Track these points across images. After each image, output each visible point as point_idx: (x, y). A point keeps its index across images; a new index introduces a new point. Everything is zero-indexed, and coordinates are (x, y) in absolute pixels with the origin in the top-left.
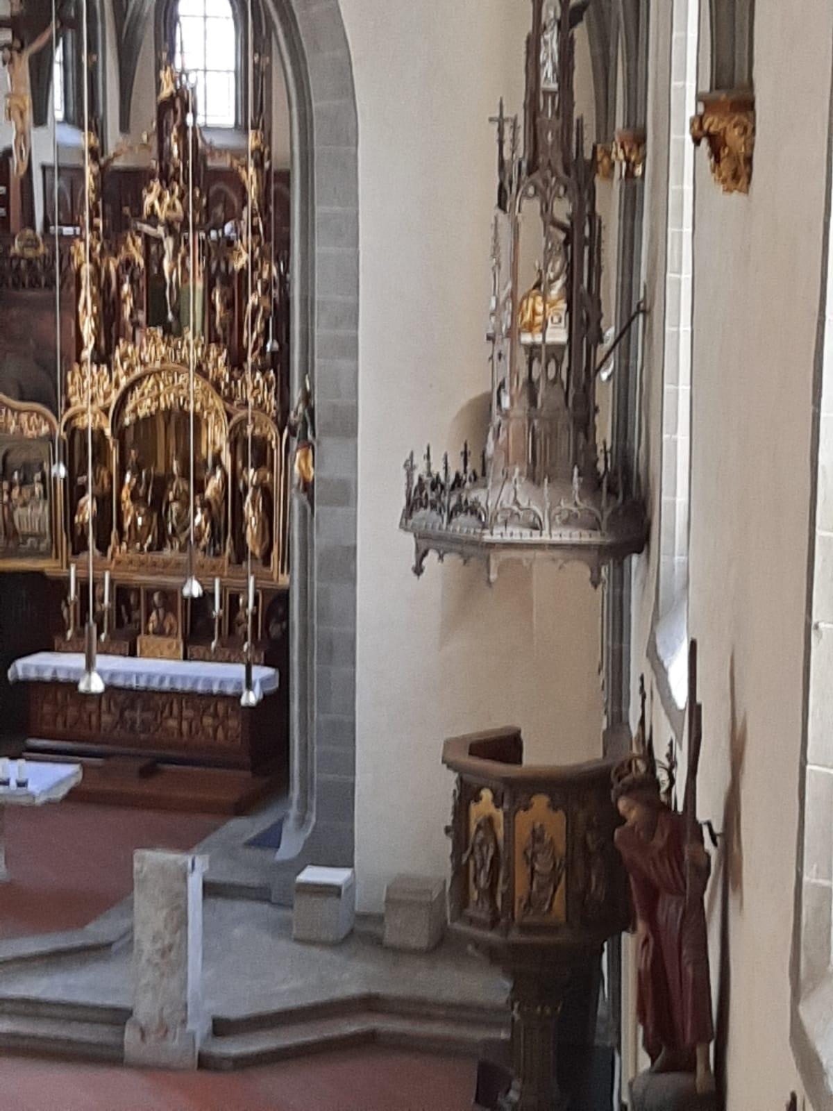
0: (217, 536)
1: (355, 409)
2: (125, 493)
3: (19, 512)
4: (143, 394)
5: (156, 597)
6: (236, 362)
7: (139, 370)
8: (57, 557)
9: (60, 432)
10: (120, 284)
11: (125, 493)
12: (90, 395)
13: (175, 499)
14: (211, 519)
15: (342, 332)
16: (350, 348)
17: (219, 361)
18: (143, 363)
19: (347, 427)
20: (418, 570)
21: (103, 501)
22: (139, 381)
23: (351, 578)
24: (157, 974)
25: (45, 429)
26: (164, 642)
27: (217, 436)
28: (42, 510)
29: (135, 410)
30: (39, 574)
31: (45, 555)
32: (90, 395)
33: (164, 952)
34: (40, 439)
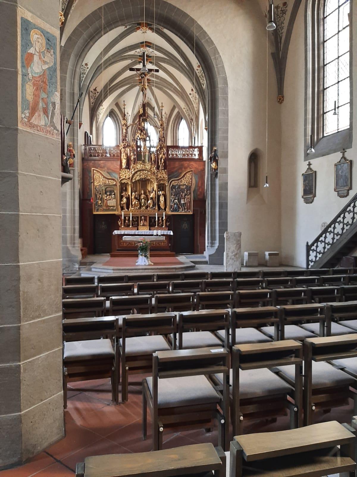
0: (154, 205)
1: (227, 152)
3: (108, 202)
4: (137, 175)
5: (143, 217)
6: (158, 168)
7: (136, 170)
9: (118, 184)
13: (143, 199)
15: (224, 135)
16: (226, 138)
18: (137, 169)
21: (128, 199)
22: (136, 172)
23: (227, 190)
24: (233, 261)
26: (145, 227)
28: (114, 200)
29: (135, 179)
30: (114, 214)
31: (115, 210)
33: (235, 255)
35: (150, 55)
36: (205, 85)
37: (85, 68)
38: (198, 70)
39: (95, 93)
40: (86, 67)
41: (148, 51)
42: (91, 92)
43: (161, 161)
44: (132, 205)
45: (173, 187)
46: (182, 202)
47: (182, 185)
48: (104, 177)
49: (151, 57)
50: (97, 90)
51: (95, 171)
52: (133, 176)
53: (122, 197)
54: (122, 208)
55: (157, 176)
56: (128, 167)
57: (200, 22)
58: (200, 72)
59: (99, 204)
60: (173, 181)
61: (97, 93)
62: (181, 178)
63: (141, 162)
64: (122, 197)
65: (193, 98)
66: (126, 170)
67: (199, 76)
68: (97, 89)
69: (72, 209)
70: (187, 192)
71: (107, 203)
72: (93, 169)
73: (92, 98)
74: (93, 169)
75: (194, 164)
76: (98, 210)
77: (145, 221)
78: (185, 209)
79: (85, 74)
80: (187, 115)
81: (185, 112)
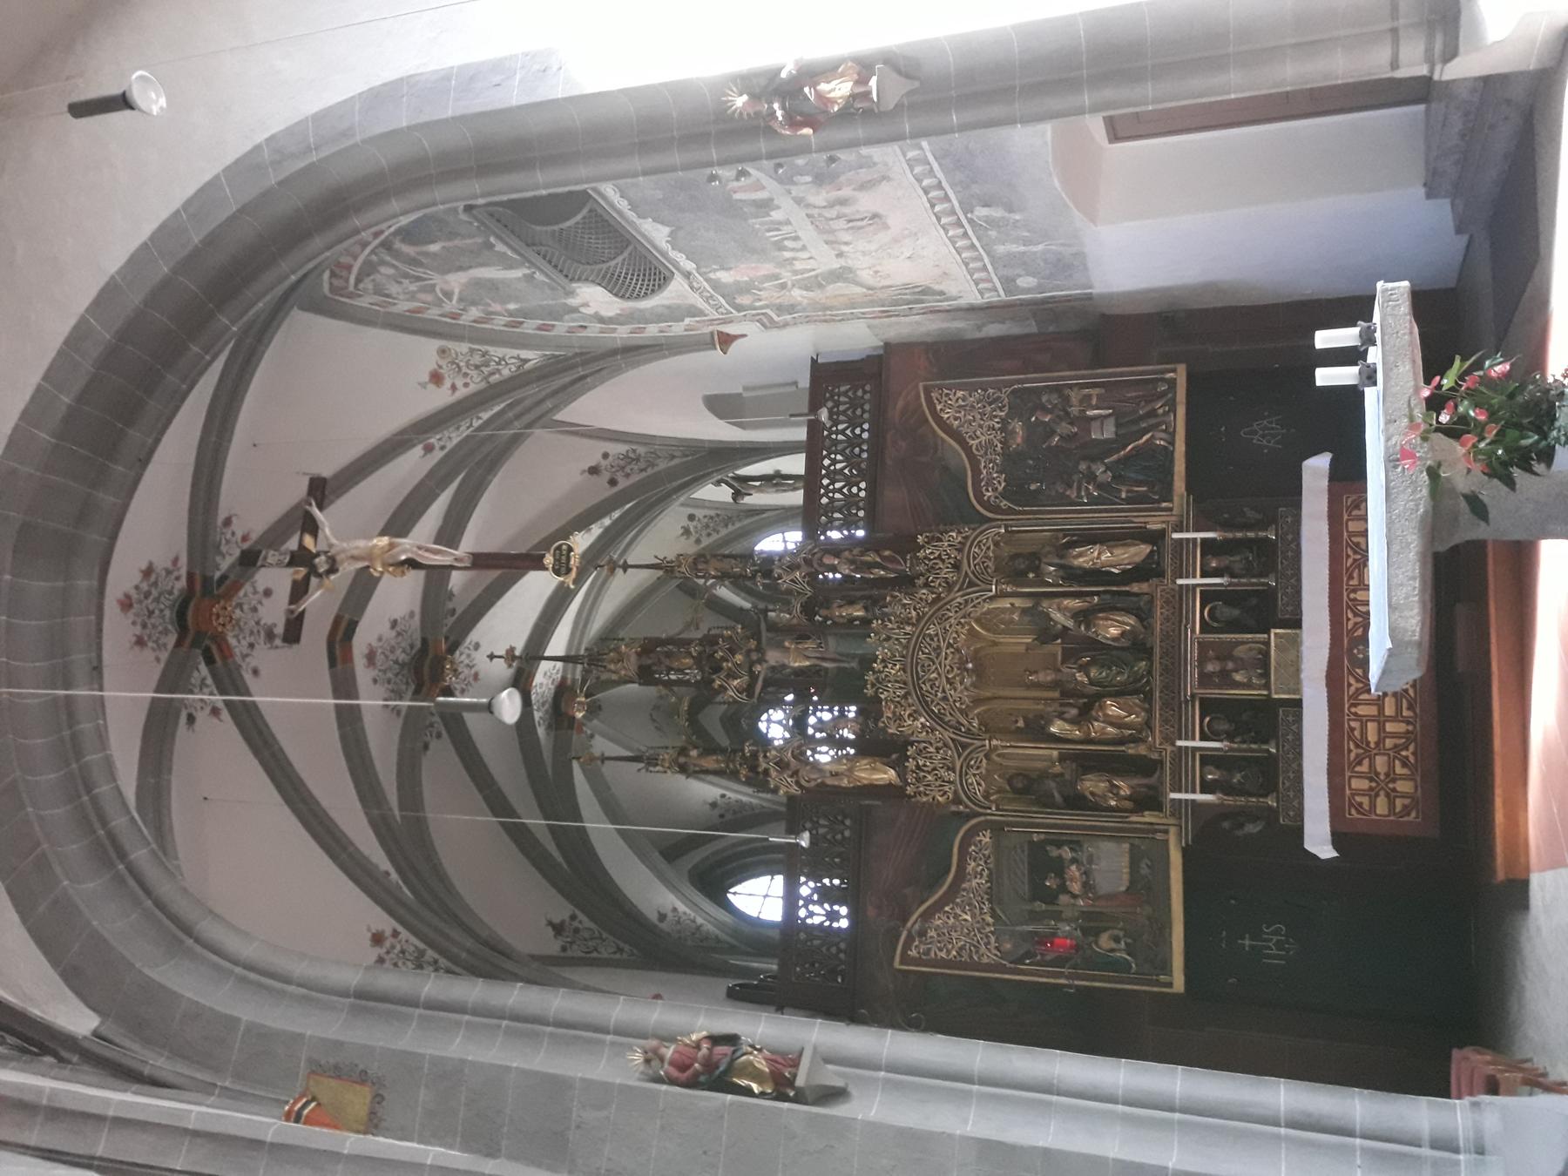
6: (906, 583)
17: (902, 604)
25: (986, 838)
34: (997, 846)
35: (418, 644)
36: (524, 354)
37: (393, 947)
38: (454, 388)
39: (577, 931)
40: (387, 944)
41: (393, 650)
42: (569, 953)
43: (870, 566)
44: (1121, 741)
45: (1018, 493)
46: (1109, 432)
47: (1004, 443)
48: (949, 897)
49: (424, 641)
50: (563, 922)
51: (913, 953)
53: (1077, 802)
55: (949, 586)
57: (114, 259)
58: (466, 375)
59: (1123, 945)
60: (979, 495)
61: (576, 924)
62: (967, 449)
63: (870, 677)
64: (1077, 802)
65: (628, 470)
66: (911, 764)
67: (483, 385)
68: (557, 920)
69: (1125, 1118)
70: (1046, 411)
71: (1111, 897)
72: (902, 963)
74: (897, 965)
75: (900, 404)
76: (1166, 967)
78: (1152, 414)
79: (422, 953)
80: (724, 532)
81: (715, 537)
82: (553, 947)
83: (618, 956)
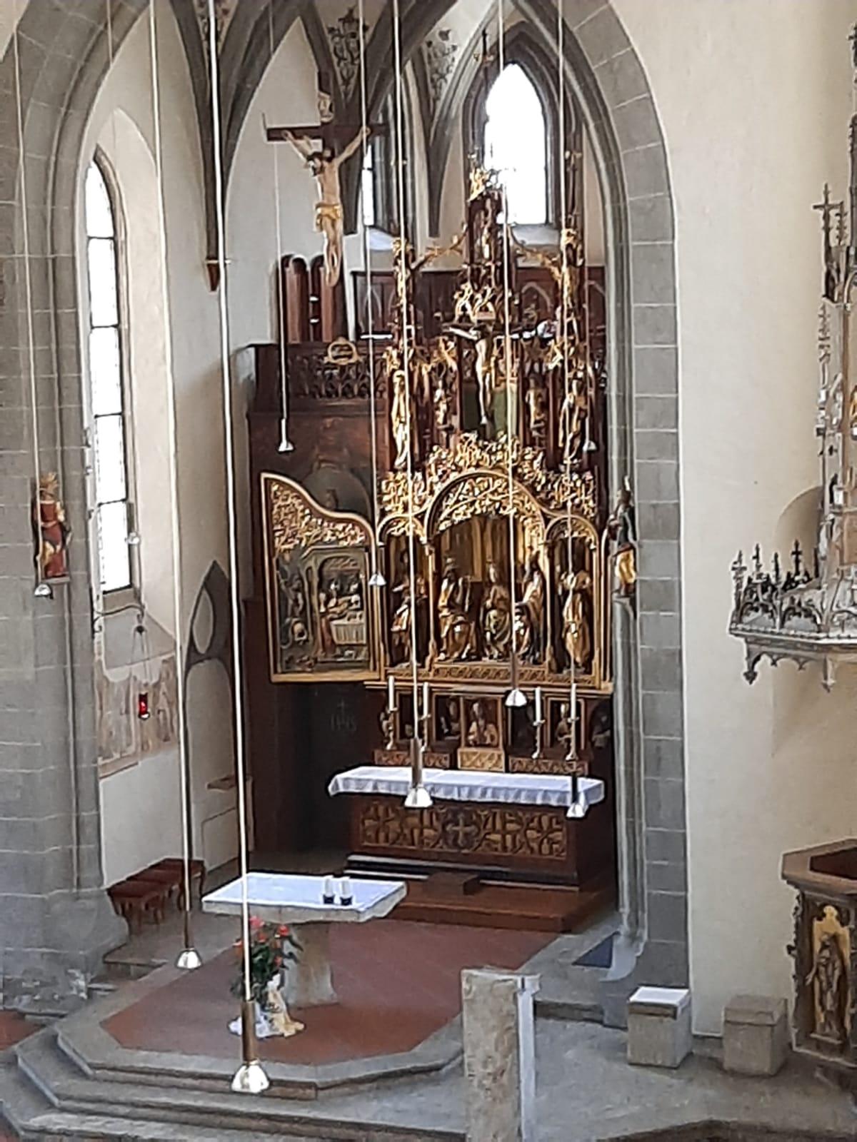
0: (536, 644)
2: (443, 601)
4: (458, 501)
5: (476, 706)
6: (553, 463)
7: (454, 476)
8: (375, 669)
9: (376, 543)
10: (433, 389)
11: (443, 601)
12: (406, 502)
13: (493, 607)
14: (529, 625)
16: (671, 446)
18: (459, 469)
19: (669, 527)
20: (751, 676)
21: (422, 608)
24: (490, 1099)
27: (533, 540)
31: (363, 666)
32: (406, 502)
33: (495, 1077)
42: (329, 36)
52: (437, 507)
54: (397, 655)
56: (418, 465)
59: (297, 639)
63: (473, 437)
72: (266, 479)
73: (341, 59)
74: (264, 475)
77: (487, 722)
82: (330, 20)
83: (340, 81)
